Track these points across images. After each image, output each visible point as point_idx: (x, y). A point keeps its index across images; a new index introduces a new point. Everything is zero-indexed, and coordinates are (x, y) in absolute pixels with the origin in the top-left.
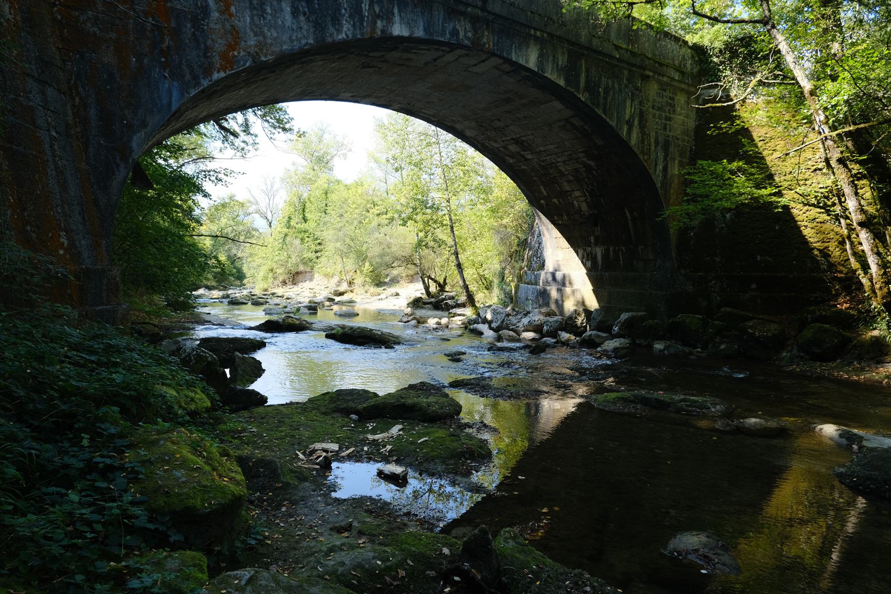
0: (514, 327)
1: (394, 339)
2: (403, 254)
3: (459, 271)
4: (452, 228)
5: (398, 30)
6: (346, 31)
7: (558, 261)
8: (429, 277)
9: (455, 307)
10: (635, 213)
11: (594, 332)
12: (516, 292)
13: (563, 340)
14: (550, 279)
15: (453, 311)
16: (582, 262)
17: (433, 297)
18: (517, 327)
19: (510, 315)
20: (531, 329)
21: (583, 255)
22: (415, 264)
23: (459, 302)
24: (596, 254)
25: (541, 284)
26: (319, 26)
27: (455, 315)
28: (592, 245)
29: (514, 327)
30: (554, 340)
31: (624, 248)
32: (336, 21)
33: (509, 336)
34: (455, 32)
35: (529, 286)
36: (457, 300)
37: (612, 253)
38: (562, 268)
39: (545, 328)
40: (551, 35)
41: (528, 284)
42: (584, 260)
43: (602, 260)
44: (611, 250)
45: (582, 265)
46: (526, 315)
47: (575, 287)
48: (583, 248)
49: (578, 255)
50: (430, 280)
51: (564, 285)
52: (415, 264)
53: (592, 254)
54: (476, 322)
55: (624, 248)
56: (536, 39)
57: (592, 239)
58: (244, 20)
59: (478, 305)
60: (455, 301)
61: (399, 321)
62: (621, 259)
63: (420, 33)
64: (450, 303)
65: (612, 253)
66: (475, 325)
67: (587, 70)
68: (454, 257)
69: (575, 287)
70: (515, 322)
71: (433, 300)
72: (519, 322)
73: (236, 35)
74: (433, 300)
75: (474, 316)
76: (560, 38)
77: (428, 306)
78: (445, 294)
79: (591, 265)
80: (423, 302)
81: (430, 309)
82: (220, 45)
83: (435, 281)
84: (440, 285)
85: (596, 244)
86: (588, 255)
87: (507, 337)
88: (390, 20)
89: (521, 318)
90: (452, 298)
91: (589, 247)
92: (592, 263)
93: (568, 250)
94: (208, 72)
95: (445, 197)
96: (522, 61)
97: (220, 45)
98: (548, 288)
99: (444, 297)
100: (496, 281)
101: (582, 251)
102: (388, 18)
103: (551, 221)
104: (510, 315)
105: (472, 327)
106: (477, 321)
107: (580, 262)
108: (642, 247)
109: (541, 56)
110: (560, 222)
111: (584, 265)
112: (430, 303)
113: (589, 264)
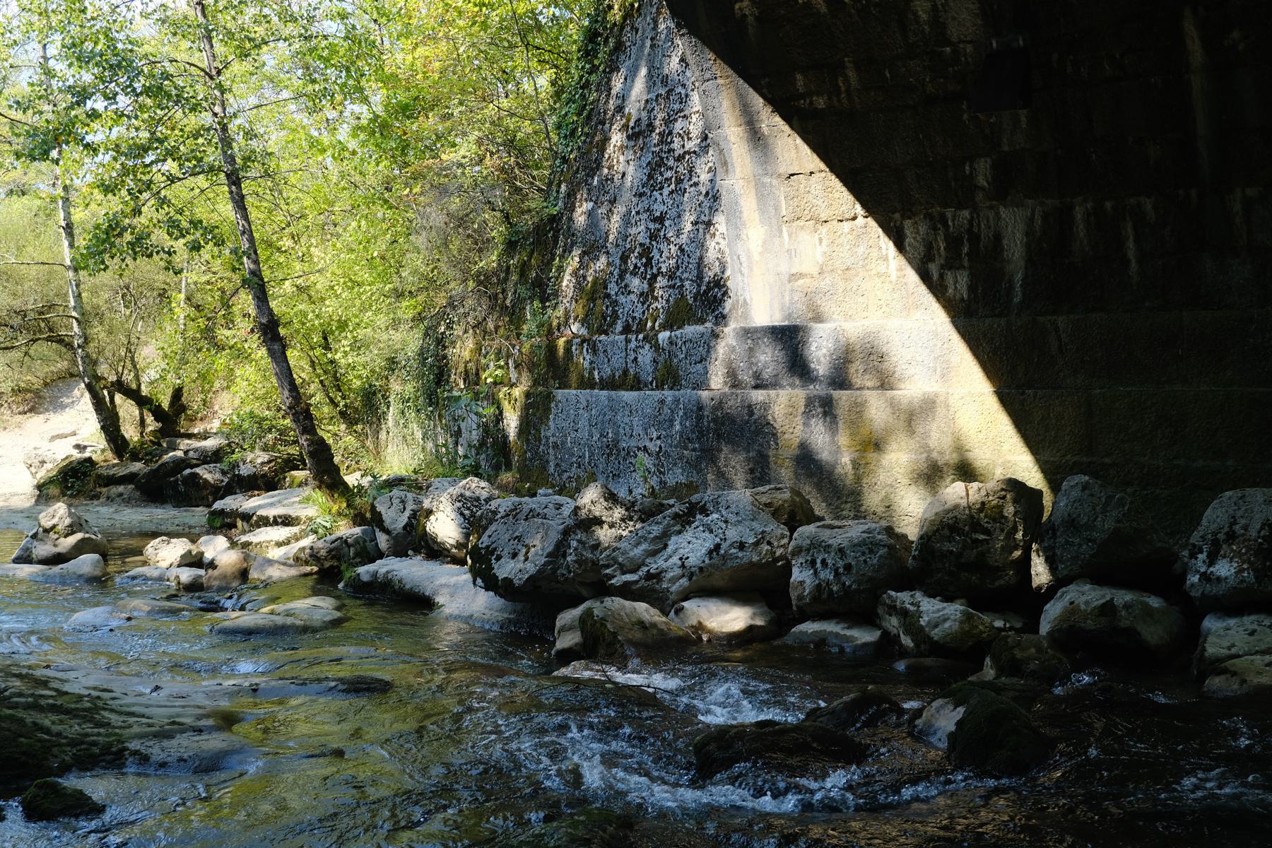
0: (630, 577)
1: (74, 728)
2: (17, 304)
3: (271, 353)
4: (234, 180)
7: (794, 277)
8: (120, 386)
9: (228, 490)
10: (1236, 34)
11: (1086, 595)
12: (526, 426)
13: (936, 634)
14: (769, 357)
15: (229, 503)
16: (925, 277)
17: (135, 457)
18: (649, 576)
19: (599, 522)
20: (721, 583)
21: (929, 247)
22: (60, 341)
23: (245, 471)
24: (998, 238)
25: (717, 381)
27: (253, 521)
28: (980, 196)
29: (630, 577)
30: (864, 636)
31: (1148, 205)
33: (642, 625)
35: (628, 396)
36: (235, 465)
37: (1081, 230)
38: (827, 307)
39: (800, 575)
41: (610, 384)
42: (934, 268)
43: (1030, 260)
44: (1079, 213)
45: (923, 289)
46: (684, 520)
47: (913, 388)
48: (929, 217)
49: (900, 246)
50: (118, 398)
51: (840, 380)
52: (60, 341)
53: (974, 238)
54: (370, 554)
55: (1148, 205)
57: (982, 172)
59: (351, 479)
60: (224, 466)
61: (18, 560)
62: (1131, 253)
64: (207, 476)
65: (1081, 230)
66: (383, 567)
68: (245, 301)
69: (913, 388)
70: (638, 551)
71: (137, 467)
72: (654, 553)
74: (137, 467)
75: (346, 530)
77: (121, 489)
78: (185, 444)
79: (972, 288)
80: (99, 476)
81: (128, 502)
83: (142, 401)
84: (158, 413)
85: (1002, 190)
86: (954, 243)
87: (638, 635)
89: (664, 537)
90: (215, 456)
91: (960, 207)
92: (973, 276)
93: (847, 225)
95: (202, 59)
98: (758, 396)
99: (180, 454)
100: (403, 388)
101: (923, 229)
103: (769, 100)
104: (599, 522)
105: (365, 571)
106: (370, 545)
107: (912, 277)
108: (1250, 192)
110: (821, 103)
111: (936, 287)
112: (130, 478)
113: (959, 283)
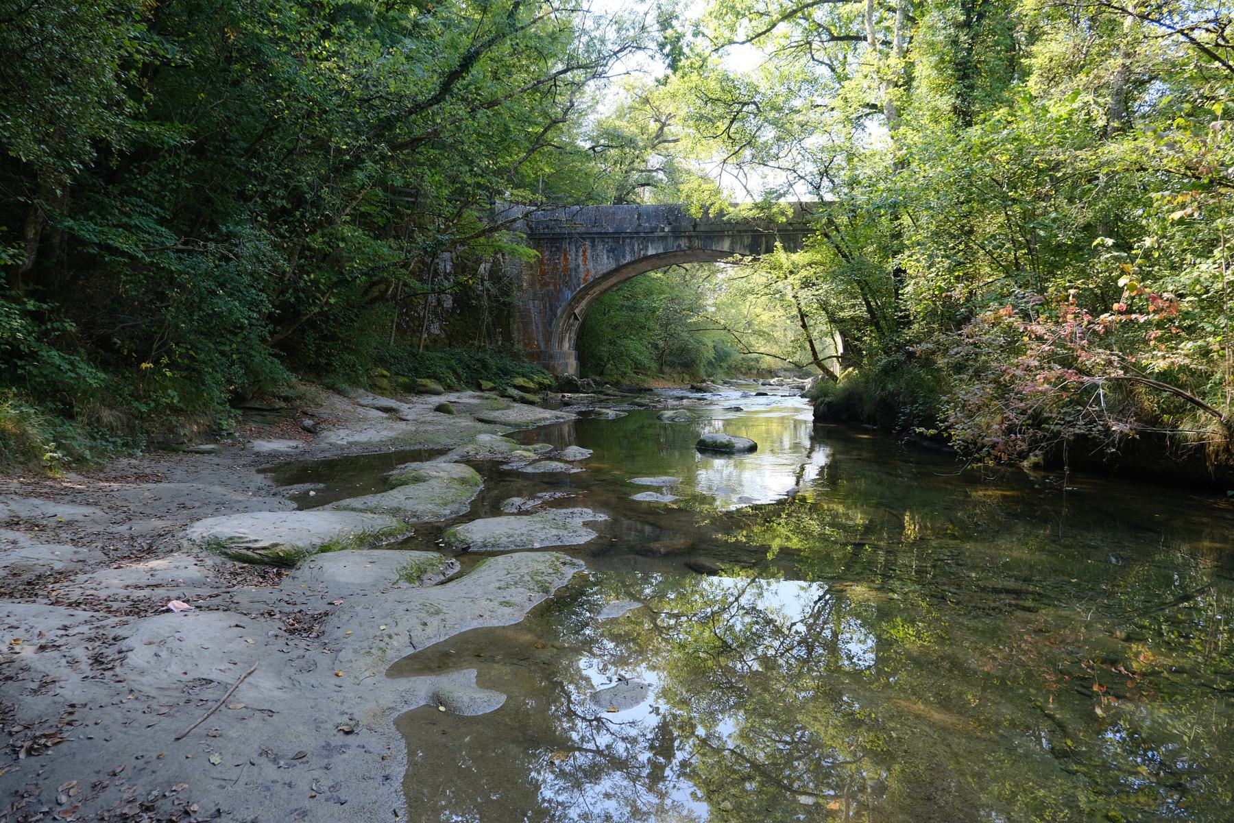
5: (651, 252)
6: (628, 258)
26: (617, 260)
32: (624, 256)
34: (679, 246)
40: (739, 231)
56: (729, 236)
58: (590, 265)
63: (661, 251)
67: (767, 242)
73: (588, 271)
76: (746, 231)
82: (583, 276)
88: (647, 250)
94: (579, 285)
96: (718, 249)
97: (583, 276)
102: (646, 248)
109: (732, 243)
